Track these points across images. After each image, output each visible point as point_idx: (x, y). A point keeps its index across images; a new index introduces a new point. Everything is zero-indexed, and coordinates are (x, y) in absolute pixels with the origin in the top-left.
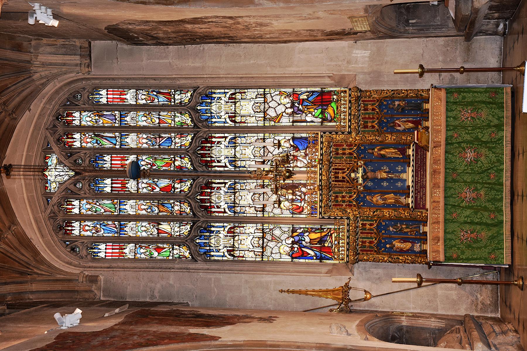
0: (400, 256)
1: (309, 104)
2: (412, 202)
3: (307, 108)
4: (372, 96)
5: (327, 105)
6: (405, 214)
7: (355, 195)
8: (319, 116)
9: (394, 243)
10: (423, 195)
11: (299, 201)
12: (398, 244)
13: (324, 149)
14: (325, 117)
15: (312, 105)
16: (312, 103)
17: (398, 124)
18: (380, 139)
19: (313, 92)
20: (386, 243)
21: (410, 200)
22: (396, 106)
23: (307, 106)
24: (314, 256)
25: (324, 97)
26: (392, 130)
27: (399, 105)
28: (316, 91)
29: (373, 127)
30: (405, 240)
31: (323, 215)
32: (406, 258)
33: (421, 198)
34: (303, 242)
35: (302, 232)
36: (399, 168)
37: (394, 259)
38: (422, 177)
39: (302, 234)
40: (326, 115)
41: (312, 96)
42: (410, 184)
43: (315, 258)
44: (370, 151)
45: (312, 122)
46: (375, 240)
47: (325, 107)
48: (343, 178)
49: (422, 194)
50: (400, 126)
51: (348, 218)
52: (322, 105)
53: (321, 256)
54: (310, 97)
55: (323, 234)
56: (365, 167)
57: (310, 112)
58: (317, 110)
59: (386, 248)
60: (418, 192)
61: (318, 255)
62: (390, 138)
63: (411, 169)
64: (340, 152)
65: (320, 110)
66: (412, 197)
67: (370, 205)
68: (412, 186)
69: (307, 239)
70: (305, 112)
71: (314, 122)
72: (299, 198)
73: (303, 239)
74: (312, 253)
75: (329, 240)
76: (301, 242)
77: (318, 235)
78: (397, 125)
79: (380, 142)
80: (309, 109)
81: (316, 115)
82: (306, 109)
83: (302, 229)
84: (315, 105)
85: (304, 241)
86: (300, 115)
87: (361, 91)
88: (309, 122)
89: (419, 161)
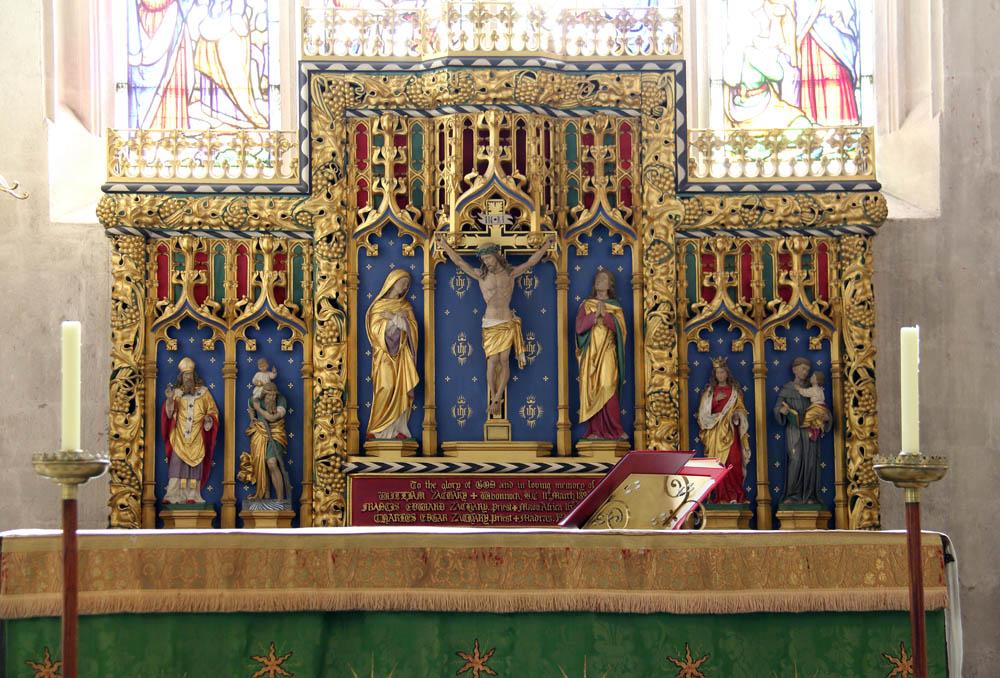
1: (801, 20)
2: (384, 467)
4: (846, 283)
6: (325, 435)
9: (203, 390)
10: (418, 513)
12: (192, 409)
18: (654, 326)
19: (855, 39)
21: (393, 458)
22: (805, 392)
26: (697, 376)
29: (709, 294)
30: (213, 439)
31: (314, 77)
32: (132, 442)
33: (402, 502)
36: (531, 411)
38: (495, 507)
48: (483, 167)
49: (421, 507)
50: (716, 408)
51: (306, 191)
55: (243, 99)
56: (533, 260)
59: (179, 354)
60: (428, 492)
62: (658, 368)
67: (366, 289)
69: (211, 29)
74: (156, 48)
78: (720, 396)
79: (644, 326)
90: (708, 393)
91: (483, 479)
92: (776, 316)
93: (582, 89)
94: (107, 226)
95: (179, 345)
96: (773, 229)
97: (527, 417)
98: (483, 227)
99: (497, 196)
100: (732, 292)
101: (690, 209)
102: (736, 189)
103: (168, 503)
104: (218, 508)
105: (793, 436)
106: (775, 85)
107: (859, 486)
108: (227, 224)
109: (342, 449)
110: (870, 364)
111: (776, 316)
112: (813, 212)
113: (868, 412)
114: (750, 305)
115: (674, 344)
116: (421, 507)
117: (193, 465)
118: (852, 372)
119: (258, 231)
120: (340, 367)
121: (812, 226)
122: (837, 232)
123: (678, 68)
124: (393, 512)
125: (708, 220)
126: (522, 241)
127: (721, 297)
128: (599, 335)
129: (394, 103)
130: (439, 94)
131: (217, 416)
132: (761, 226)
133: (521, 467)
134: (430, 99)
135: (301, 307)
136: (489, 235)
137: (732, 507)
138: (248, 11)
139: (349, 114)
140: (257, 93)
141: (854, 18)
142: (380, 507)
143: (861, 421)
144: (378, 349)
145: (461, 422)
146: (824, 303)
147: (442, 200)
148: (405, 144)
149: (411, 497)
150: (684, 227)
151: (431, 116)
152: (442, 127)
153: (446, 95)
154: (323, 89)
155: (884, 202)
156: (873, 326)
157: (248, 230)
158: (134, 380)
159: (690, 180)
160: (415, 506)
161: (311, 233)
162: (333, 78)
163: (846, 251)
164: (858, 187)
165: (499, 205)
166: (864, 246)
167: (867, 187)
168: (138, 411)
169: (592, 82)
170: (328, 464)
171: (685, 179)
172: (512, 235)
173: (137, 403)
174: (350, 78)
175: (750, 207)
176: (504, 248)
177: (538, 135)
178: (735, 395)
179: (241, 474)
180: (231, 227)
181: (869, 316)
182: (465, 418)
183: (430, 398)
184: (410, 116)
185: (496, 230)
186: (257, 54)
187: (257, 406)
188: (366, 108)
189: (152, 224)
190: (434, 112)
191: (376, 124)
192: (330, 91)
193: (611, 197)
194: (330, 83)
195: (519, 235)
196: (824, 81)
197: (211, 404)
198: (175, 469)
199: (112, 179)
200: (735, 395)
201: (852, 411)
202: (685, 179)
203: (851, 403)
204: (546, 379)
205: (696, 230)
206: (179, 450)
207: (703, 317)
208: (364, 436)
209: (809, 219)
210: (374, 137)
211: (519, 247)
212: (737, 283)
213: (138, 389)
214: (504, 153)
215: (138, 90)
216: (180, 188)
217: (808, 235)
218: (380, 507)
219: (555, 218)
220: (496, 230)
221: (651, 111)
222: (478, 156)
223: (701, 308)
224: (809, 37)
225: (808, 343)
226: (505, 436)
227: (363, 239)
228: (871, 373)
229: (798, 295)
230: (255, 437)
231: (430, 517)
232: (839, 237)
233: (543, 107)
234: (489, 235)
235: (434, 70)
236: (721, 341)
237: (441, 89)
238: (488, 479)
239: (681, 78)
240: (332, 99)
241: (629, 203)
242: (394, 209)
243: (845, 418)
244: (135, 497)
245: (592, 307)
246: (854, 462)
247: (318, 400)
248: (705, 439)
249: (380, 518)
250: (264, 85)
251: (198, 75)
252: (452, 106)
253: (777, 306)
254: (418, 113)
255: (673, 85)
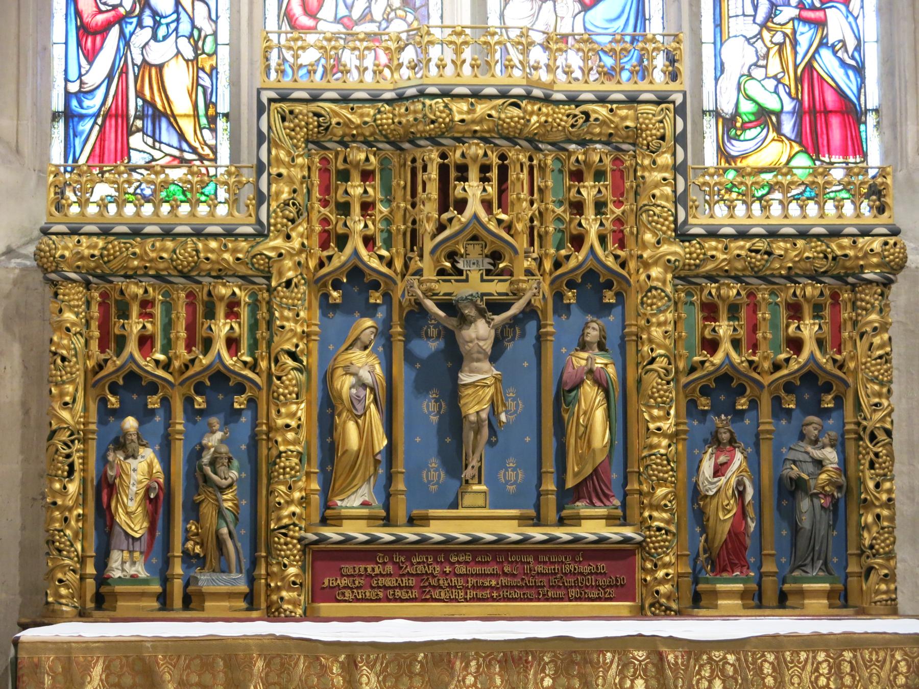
0: (84, 481)
1: (801, 50)
2: (348, 539)
3: (781, 45)
4: (862, 335)
5: (799, 139)
7: (375, 263)
8: (749, 98)
11: (343, 12)
13: (602, 111)
14: (744, 128)
15: (796, 67)
16: (809, 67)
17: (726, 465)
19: (859, 70)
20: (144, 416)
21: (358, 531)
22: (817, 453)
23: (795, 44)
24: (82, 83)
25: (835, 122)
27: (819, 464)
28: (861, 86)
29: (712, 345)
31: (273, 105)
32: (70, 509)
34: (148, 32)
35: (194, 26)
36: (511, 475)
37: (68, 456)
38: (472, 581)
39: (185, 28)
40: (750, 134)
41: (843, 63)
42: (435, 532)
43: (74, 88)
44: (593, 334)
45: (720, 68)
46: (157, 362)
47: (788, 126)
48: (461, 205)
49: (388, 582)
50: (719, 471)
52: (799, 113)
53: (82, 117)
54: (835, 53)
55: (187, 126)
57: (766, 56)
58: (776, 92)
59: (120, 414)
61: (86, 103)
63: (512, 532)
64: (589, 191)
65: (772, 103)
66: (374, 540)
68: (424, 540)
69: (158, 53)
70: (765, 33)
71: (717, 80)
72: (356, 14)
73: (162, 31)
74: (97, 73)
75: (157, 154)
76: (148, 21)
77: (181, 104)
78: (722, 459)
80: (780, 52)
81: (752, 88)
82: (779, 38)
83: (208, 28)
84: (799, 80)
85: (154, 37)
86: (749, 10)
87: (887, 283)
88: (717, 54)
89: (547, 569)
90: (707, 456)
91: (458, 552)
92: (785, 372)
93: (571, 121)
94: (45, 271)
95: (207, 402)
96: (781, 276)
97: (507, 482)
98: (460, 272)
99: (475, 238)
100: (736, 343)
101: (691, 253)
102: (742, 234)
103: (110, 577)
104: (166, 580)
105: (805, 504)
106: (774, 119)
107: (874, 556)
108: (175, 268)
109: (300, 517)
110: (888, 426)
111: (785, 372)
112: (826, 257)
113: (885, 475)
114: (756, 358)
115: (671, 401)
116: (388, 582)
117: (137, 536)
118: (868, 431)
119: (209, 275)
120: (299, 426)
121: (825, 272)
122: (851, 280)
123: (679, 99)
124: (357, 588)
125: (710, 266)
126: (503, 287)
127: (726, 346)
128: (590, 393)
129: (363, 135)
130: (412, 126)
131: (162, 480)
132: (768, 272)
133: (501, 540)
134: (402, 131)
135: (256, 360)
136: (467, 280)
137: (735, 580)
138: (196, 33)
139: (311, 146)
140: (204, 121)
141: (858, 48)
142: (343, 582)
143: (877, 486)
144: (340, 407)
145: (433, 488)
146: (838, 357)
147: (414, 242)
148: (374, 180)
149: (377, 571)
150: (682, 274)
151: (402, 149)
152: (414, 160)
153: (420, 127)
154: (284, 119)
155: (904, 248)
156: (890, 382)
157: (198, 275)
158: (73, 441)
159: (691, 221)
160: (382, 581)
161: (269, 278)
162: (298, 108)
163: (862, 300)
164: (877, 231)
165: (478, 248)
166: (882, 294)
167: (884, 231)
168: (77, 475)
169: (583, 113)
170: (285, 535)
171: (685, 222)
172: (492, 281)
173: (77, 467)
174: (314, 107)
175: (757, 251)
176: (483, 295)
177: (522, 170)
178: (739, 457)
179: (190, 545)
180: (180, 272)
181: (886, 371)
182: (437, 483)
183: (400, 466)
184: (378, 149)
185: (475, 276)
186: (206, 81)
187: (208, 470)
188: (330, 140)
189: (94, 269)
190: (406, 146)
191: (341, 158)
192: (291, 121)
193: (602, 239)
194: (291, 112)
195: (500, 281)
196: (827, 112)
197: (157, 467)
198: (118, 539)
199: (52, 220)
200: (739, 457)
201: (868, 473)
202: (685, 222)
203: (867, 465)
204: (528, 439)
205: (697, 276)
206: (121, 518)
207: (705, 372)
208: (327, 505)
209: (822, 265)
210: (338, 172)
211: (499, 294)
212: (742, 333)
213: (78, 451)
214: (484, 190)
215: (76, 119)
216: (124, 229)
217: (821, 282)
218: (343, 582)
219: (540, 262)
220: (475, 276)
221: (648, 145)
222: (458, 193)
223: (703, 363)
224: (809, 67)
225: (820, 401)
226: (481, 502)
227: (325, 285)
228: (889, 433)
229: (810, 347)
230: (204, 505)
231: (398, 593)
232: (854, 286)
233: (530, 141)
234: (467, 280)
235: (407, 99)
236: (722, 398)
237: (416, 119)
238: (465, 551)
239: (680, 111)
240: (293, 130)
241: (622, 246)
242: (363, 252)
243: (861, 482)
244: (74, 571)
245: (580, 360)
246: (869, 531)
247: (275, 464)
248: (705, 505)
249: (343, 594)
250: (211, 111)
251: (140, 102)
252: (426, 139)
253: (787, 360)
254: (388, 146)
255: (671, 115)
